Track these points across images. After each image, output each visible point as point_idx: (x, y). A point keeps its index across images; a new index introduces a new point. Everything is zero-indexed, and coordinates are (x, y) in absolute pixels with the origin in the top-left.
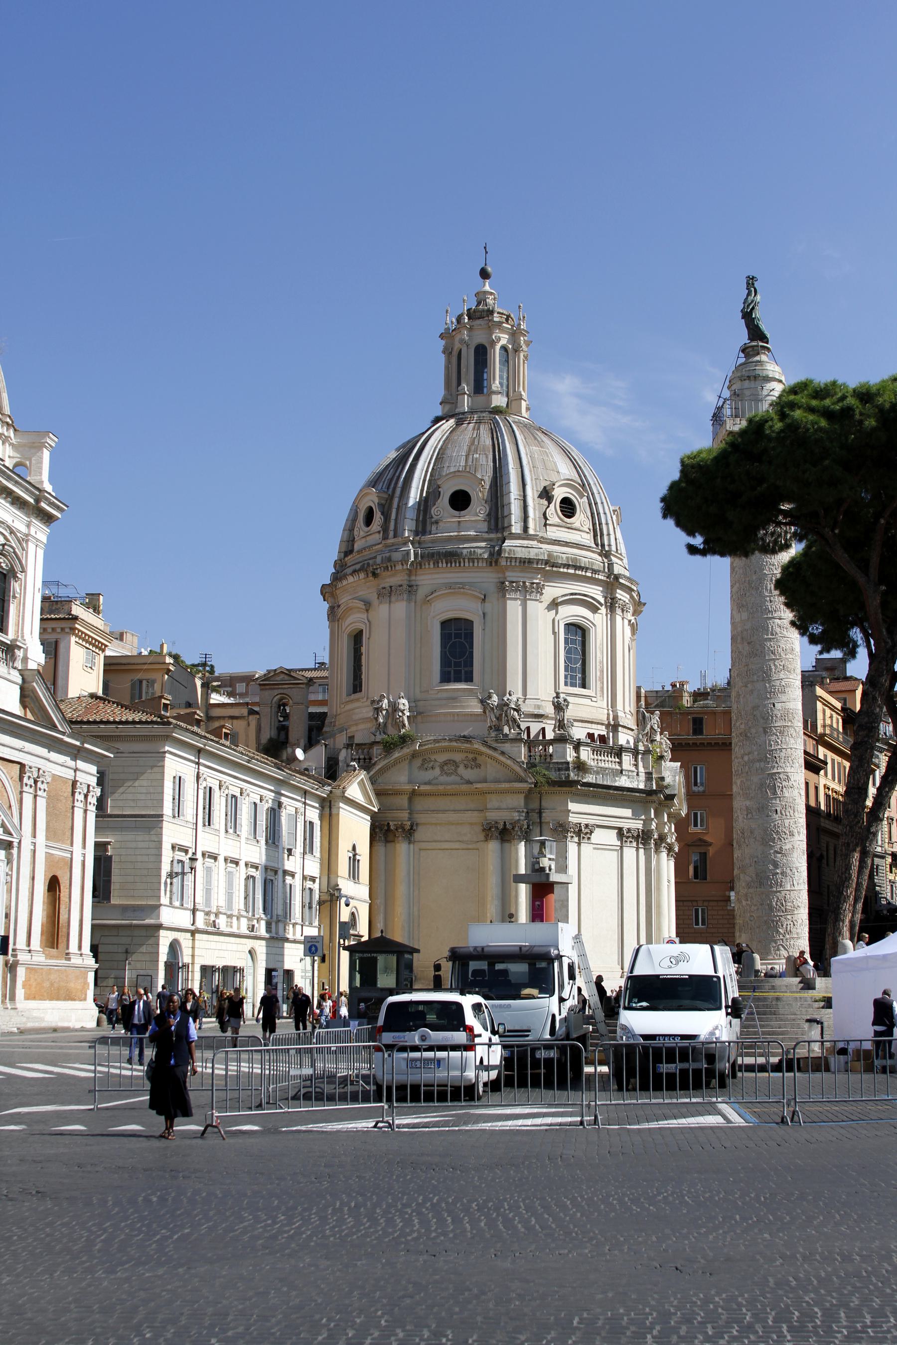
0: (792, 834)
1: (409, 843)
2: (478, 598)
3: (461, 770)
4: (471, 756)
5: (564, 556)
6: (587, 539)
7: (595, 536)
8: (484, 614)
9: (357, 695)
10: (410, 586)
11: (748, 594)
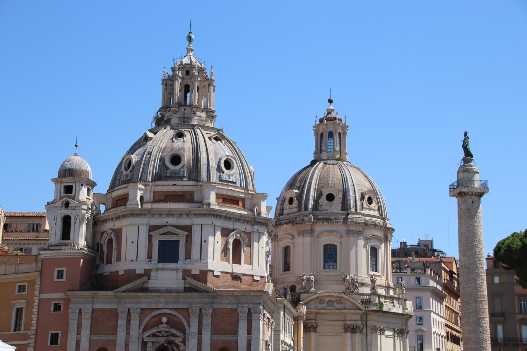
0: (486, 341)
1: (315, 333)
2: (339, 236)
3: (335, 304)
4: (339, 299)
5: (370, 220)
6: (376, 213)
7: (379, 211)
8: (341, 243)
9: (288, 272)
10: (312, 231)
11: (467, 251)
